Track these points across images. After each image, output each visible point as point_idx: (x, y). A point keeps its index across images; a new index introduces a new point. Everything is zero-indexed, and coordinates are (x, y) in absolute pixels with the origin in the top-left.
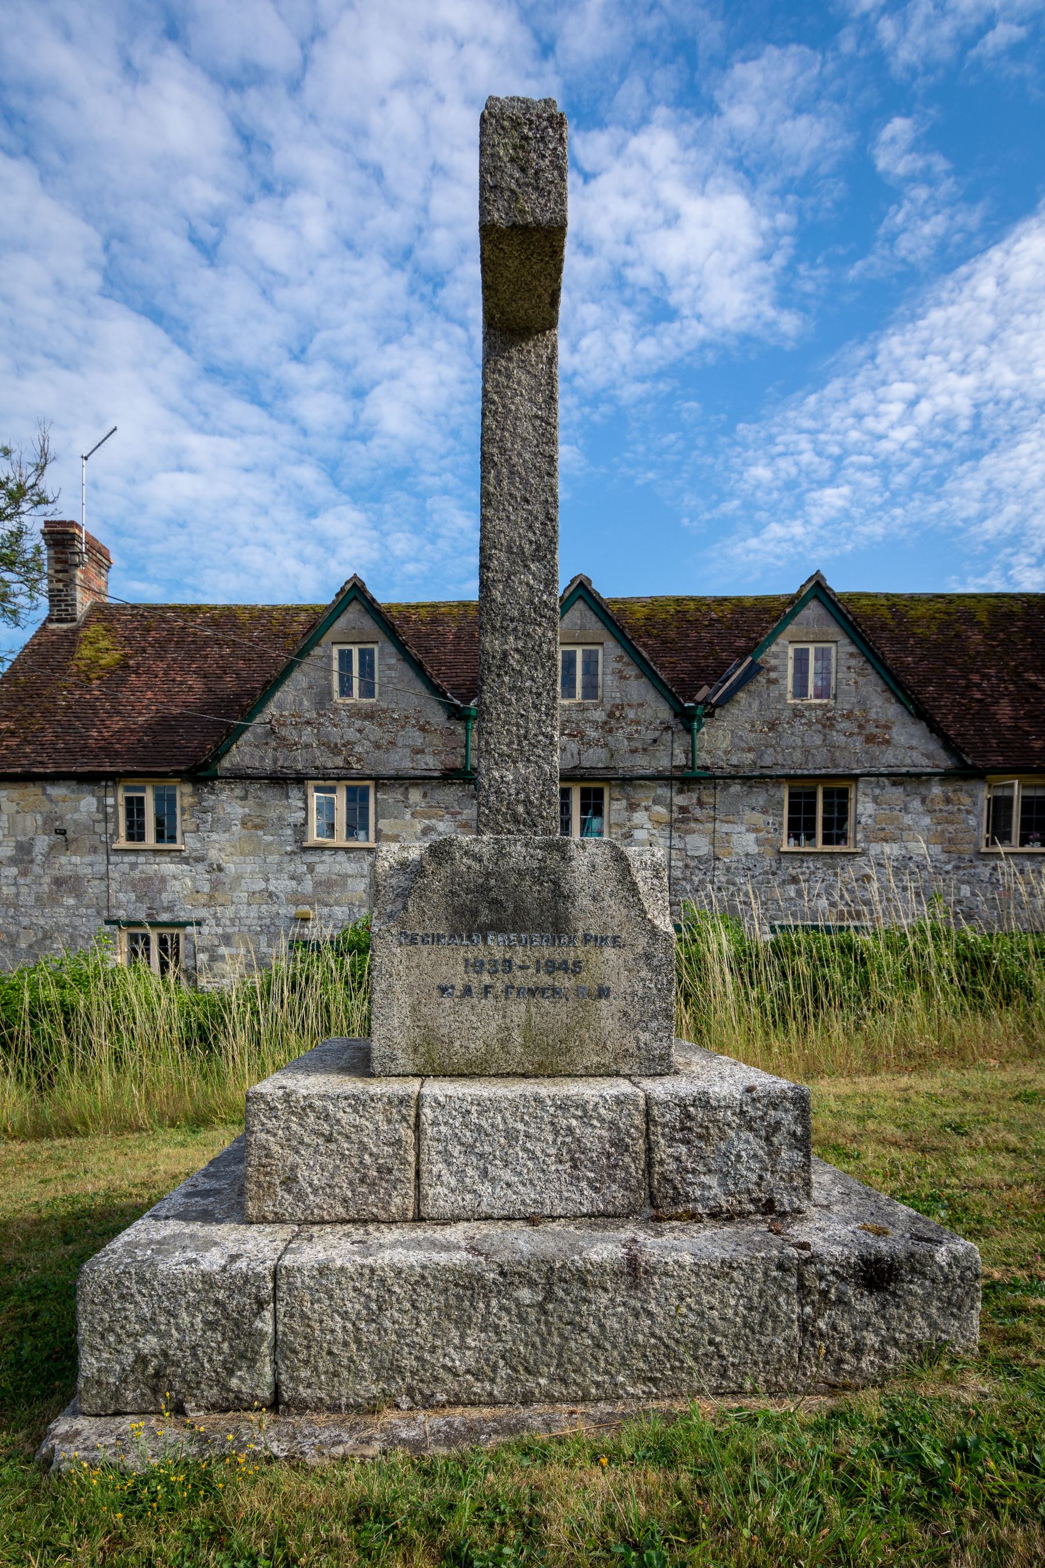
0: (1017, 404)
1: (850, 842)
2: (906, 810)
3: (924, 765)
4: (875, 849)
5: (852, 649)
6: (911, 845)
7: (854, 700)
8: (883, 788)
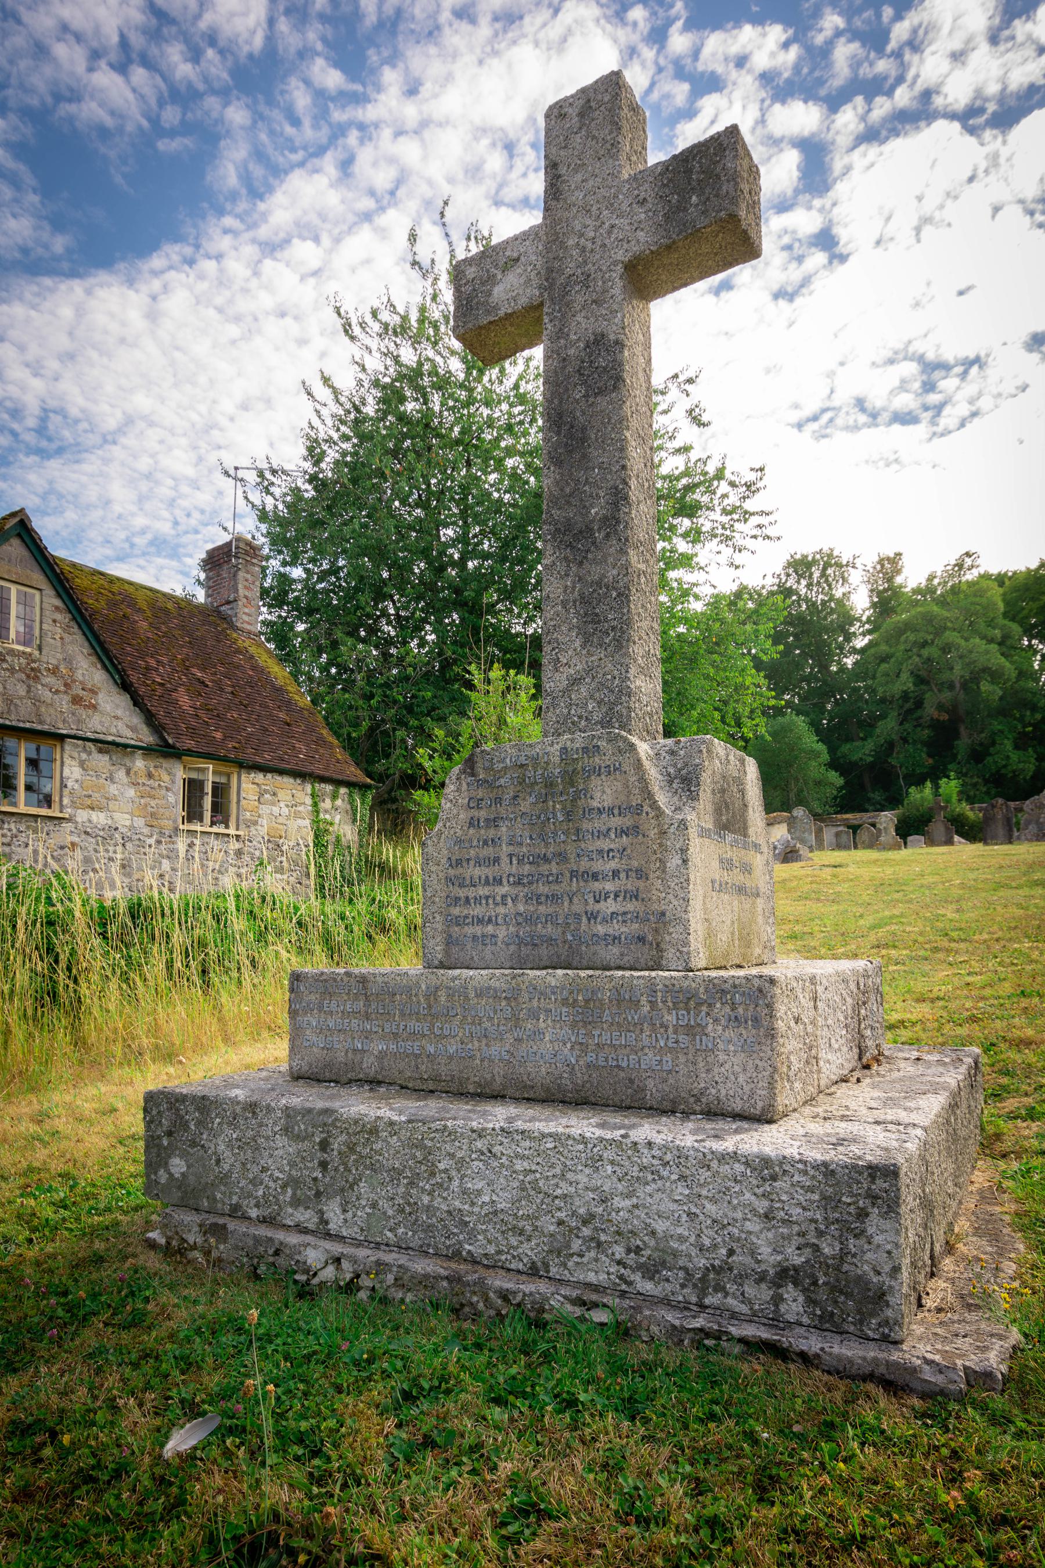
0: (84, 425)
1: (56, 806)
2: (111, 778)
3: (128, 736)
4: (82, 816)
5: (58, 602)
6: (117, 816)
7: (59, 656)
8: (90, 753)
